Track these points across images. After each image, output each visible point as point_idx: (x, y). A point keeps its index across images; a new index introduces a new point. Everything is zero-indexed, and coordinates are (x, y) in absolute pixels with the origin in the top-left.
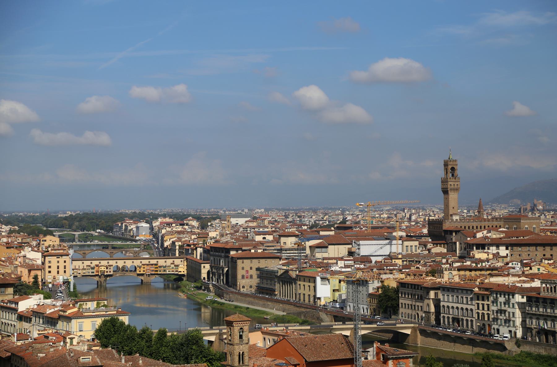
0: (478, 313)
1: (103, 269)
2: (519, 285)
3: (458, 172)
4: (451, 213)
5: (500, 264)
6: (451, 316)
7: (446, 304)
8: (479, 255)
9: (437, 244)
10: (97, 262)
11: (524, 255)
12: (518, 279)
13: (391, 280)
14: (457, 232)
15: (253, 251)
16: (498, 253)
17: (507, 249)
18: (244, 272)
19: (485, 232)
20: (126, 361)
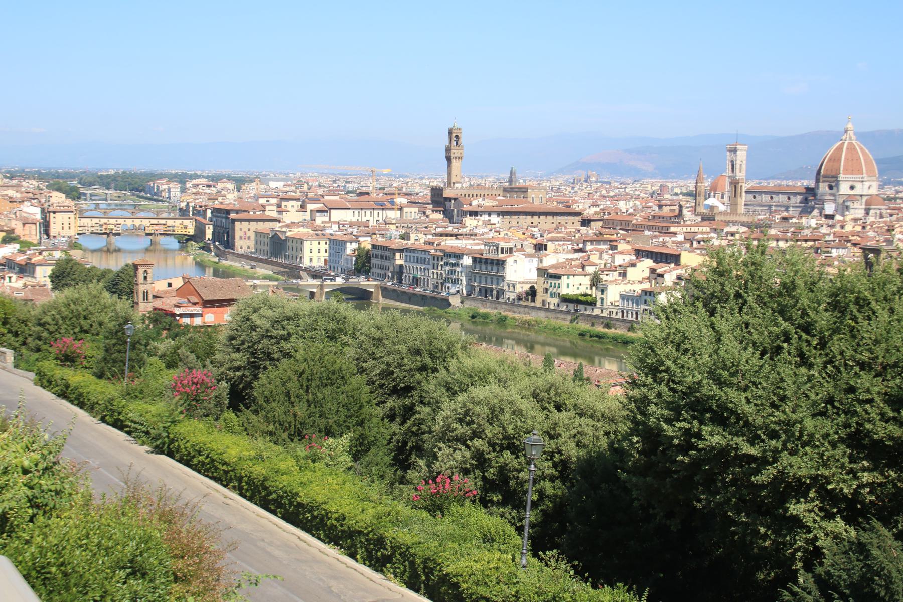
1: (111, 227)
2: (469, 247)
3: (462, 141)
4: (453, 180)
8: (470, 221)
9: (436, 211)
10: (105, 220)
11: (514, 223)
13: (367, 243)
14: (455, 199)
15: (251, 213)
16: (489, 220)
18: (242, 234)
19: (480, 200)
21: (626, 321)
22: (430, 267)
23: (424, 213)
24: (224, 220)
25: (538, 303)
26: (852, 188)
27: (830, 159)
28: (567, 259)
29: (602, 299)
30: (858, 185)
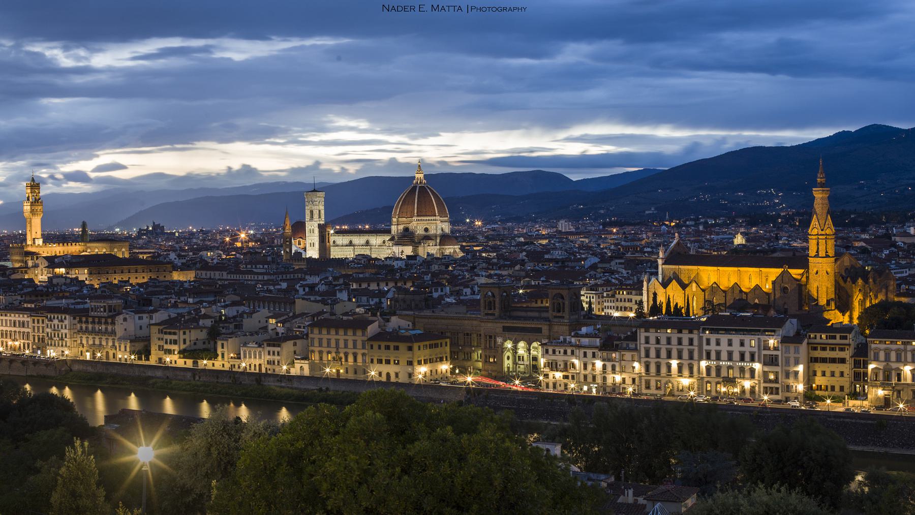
2: (72, 307)
12: (73, 301)
25: (153, 361)
28: (178, 314)
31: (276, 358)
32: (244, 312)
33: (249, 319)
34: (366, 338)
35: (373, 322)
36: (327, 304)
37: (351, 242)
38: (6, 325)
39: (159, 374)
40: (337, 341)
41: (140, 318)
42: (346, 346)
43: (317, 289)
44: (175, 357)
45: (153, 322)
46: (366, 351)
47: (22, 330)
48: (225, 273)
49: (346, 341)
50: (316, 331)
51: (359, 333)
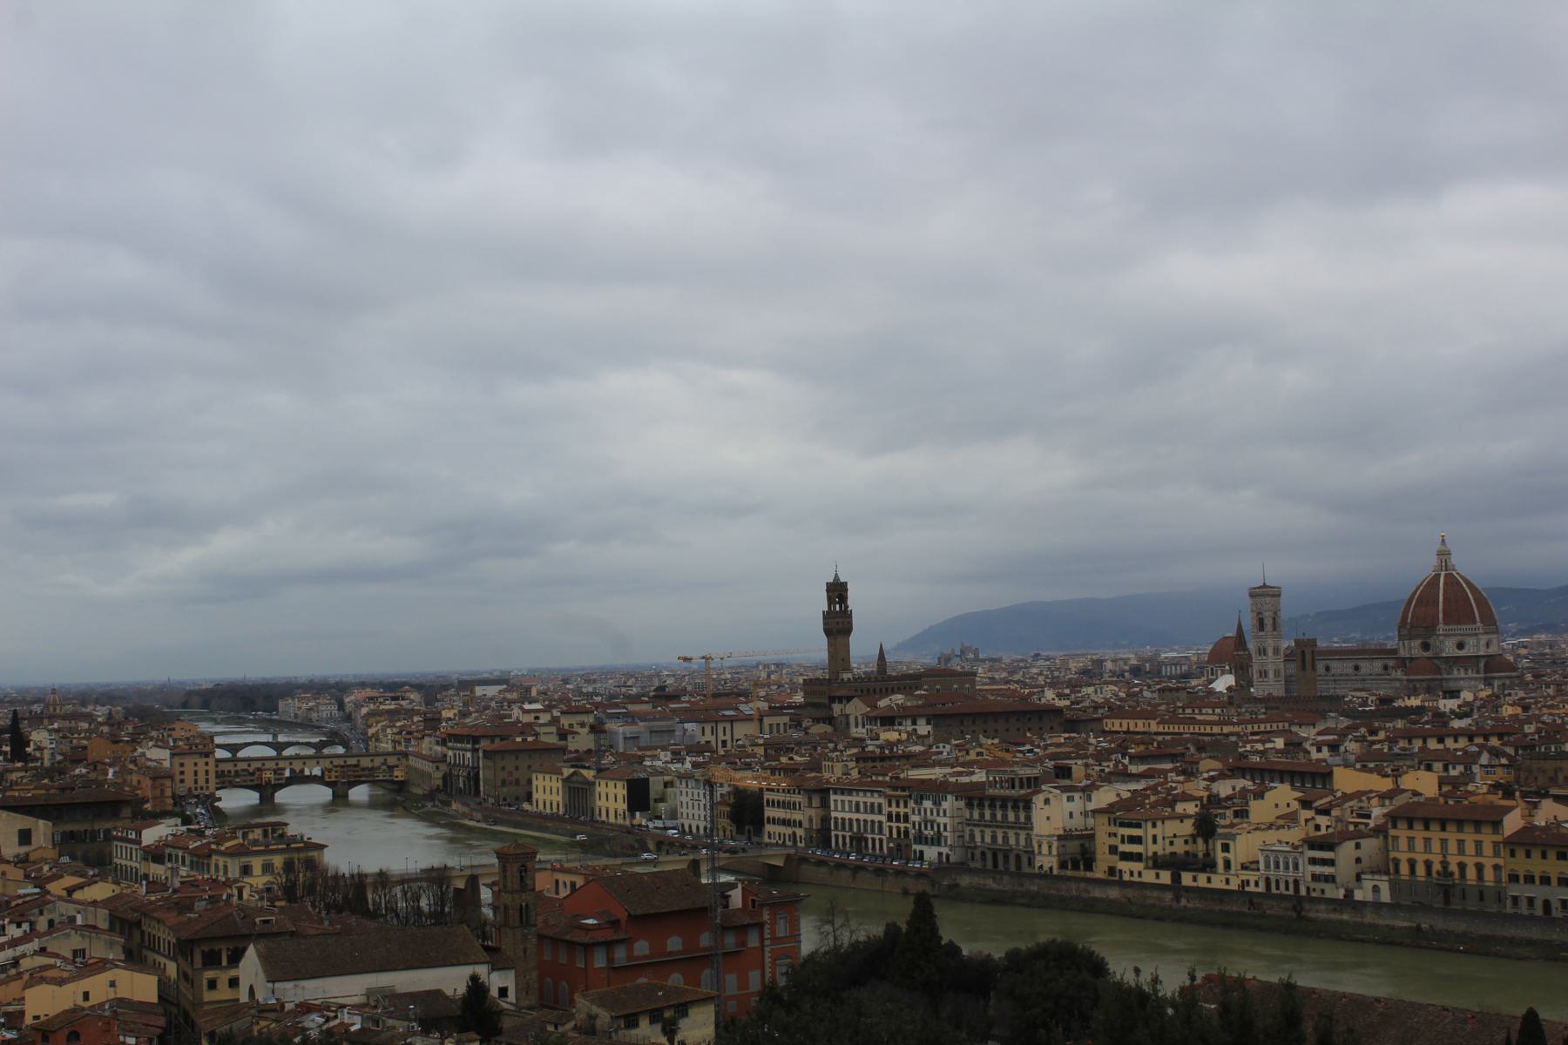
0: (891, 829)
2: (952, 779)
5: (918, 749)
6: (848, 834)
7: (839, 815)
17: (928, 723)
20: (331, 924)
21: (1282, 897)
22: (883, 818)
23: (799, 724)
24: (469, 755)
25: (1099, 872)
26: (1460, 646)
27: (1419, 601)
29: (1227, 864)
30: (1471, 641)
31: (1327, 870)
32: (1244, 789)
33: (1260, 802)
34: (1498, 838)
35: (1509, 809)
36: (1386, 776)
37: (1328, 669)
38: (843, 810)
39: (1114, 893)
40: (1444, 841)
41: (1070, 799)
42: (1461, 851)
43: (1342, 749)
44: (1137, 866)
45: (1091, 806)
46: (1500, 861)
47: (870, 817)
48: (1153, 723)
49: (1461, 843)
50: (1402, 825)
51: (1487, 829)
